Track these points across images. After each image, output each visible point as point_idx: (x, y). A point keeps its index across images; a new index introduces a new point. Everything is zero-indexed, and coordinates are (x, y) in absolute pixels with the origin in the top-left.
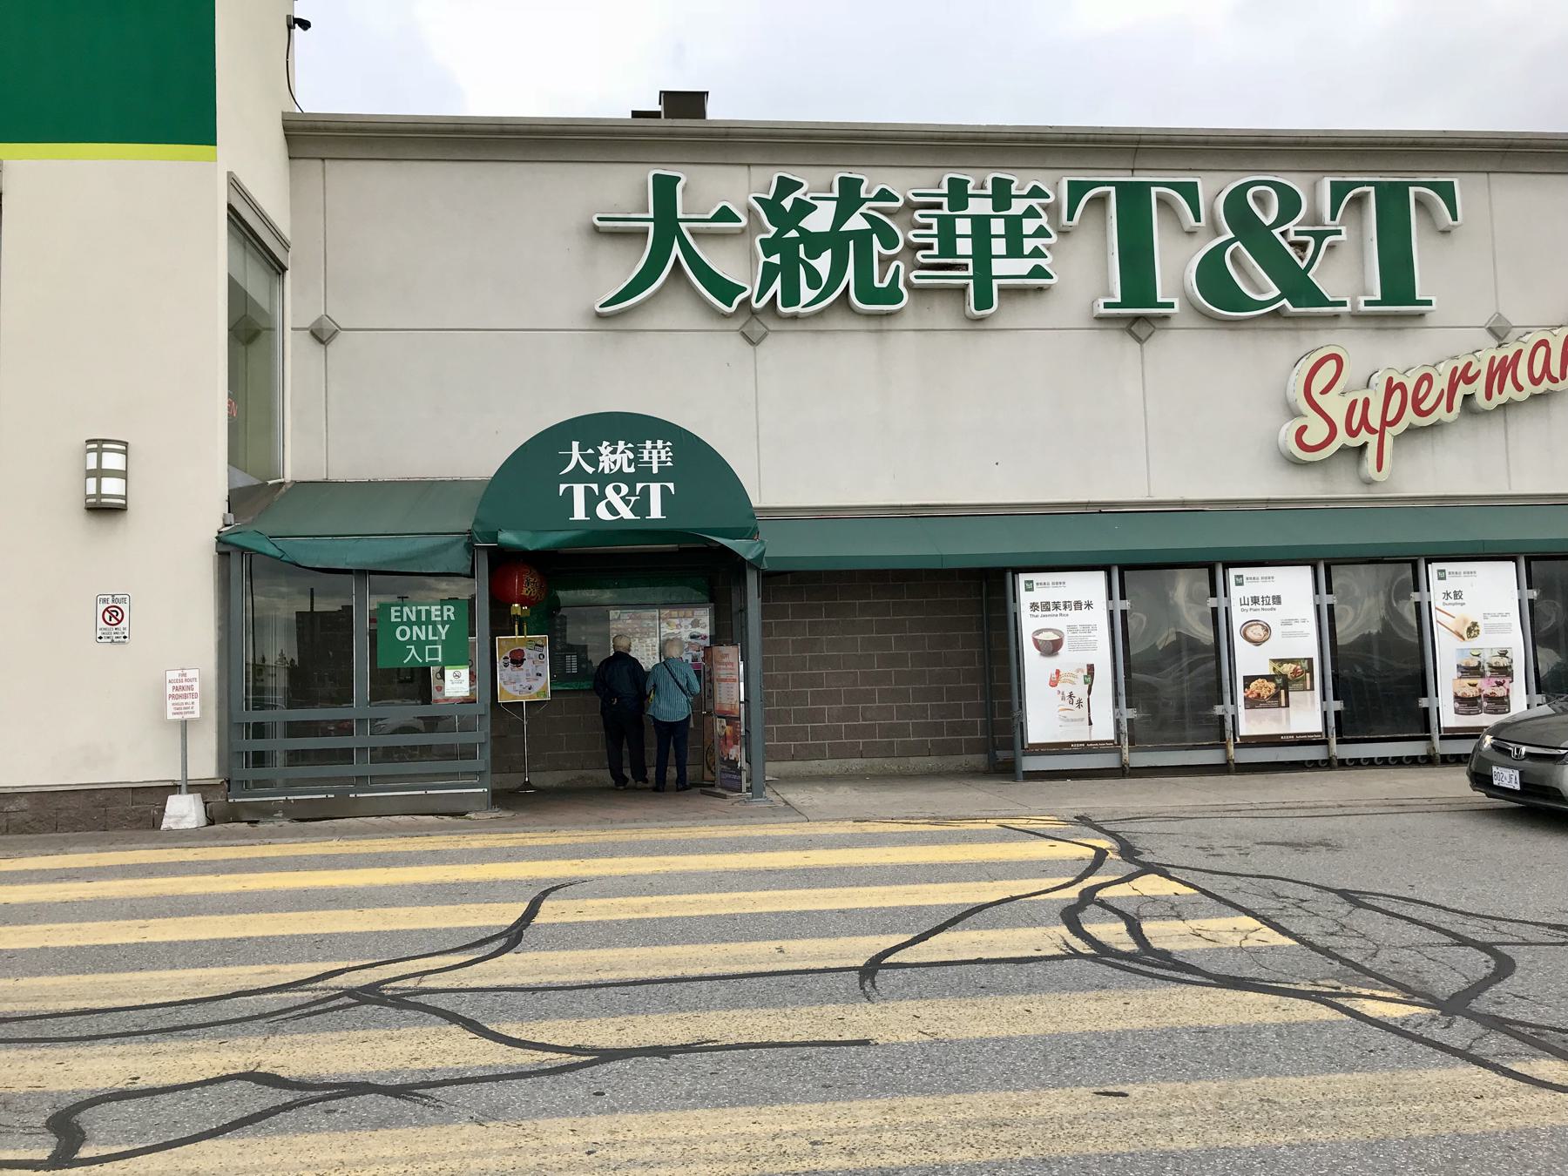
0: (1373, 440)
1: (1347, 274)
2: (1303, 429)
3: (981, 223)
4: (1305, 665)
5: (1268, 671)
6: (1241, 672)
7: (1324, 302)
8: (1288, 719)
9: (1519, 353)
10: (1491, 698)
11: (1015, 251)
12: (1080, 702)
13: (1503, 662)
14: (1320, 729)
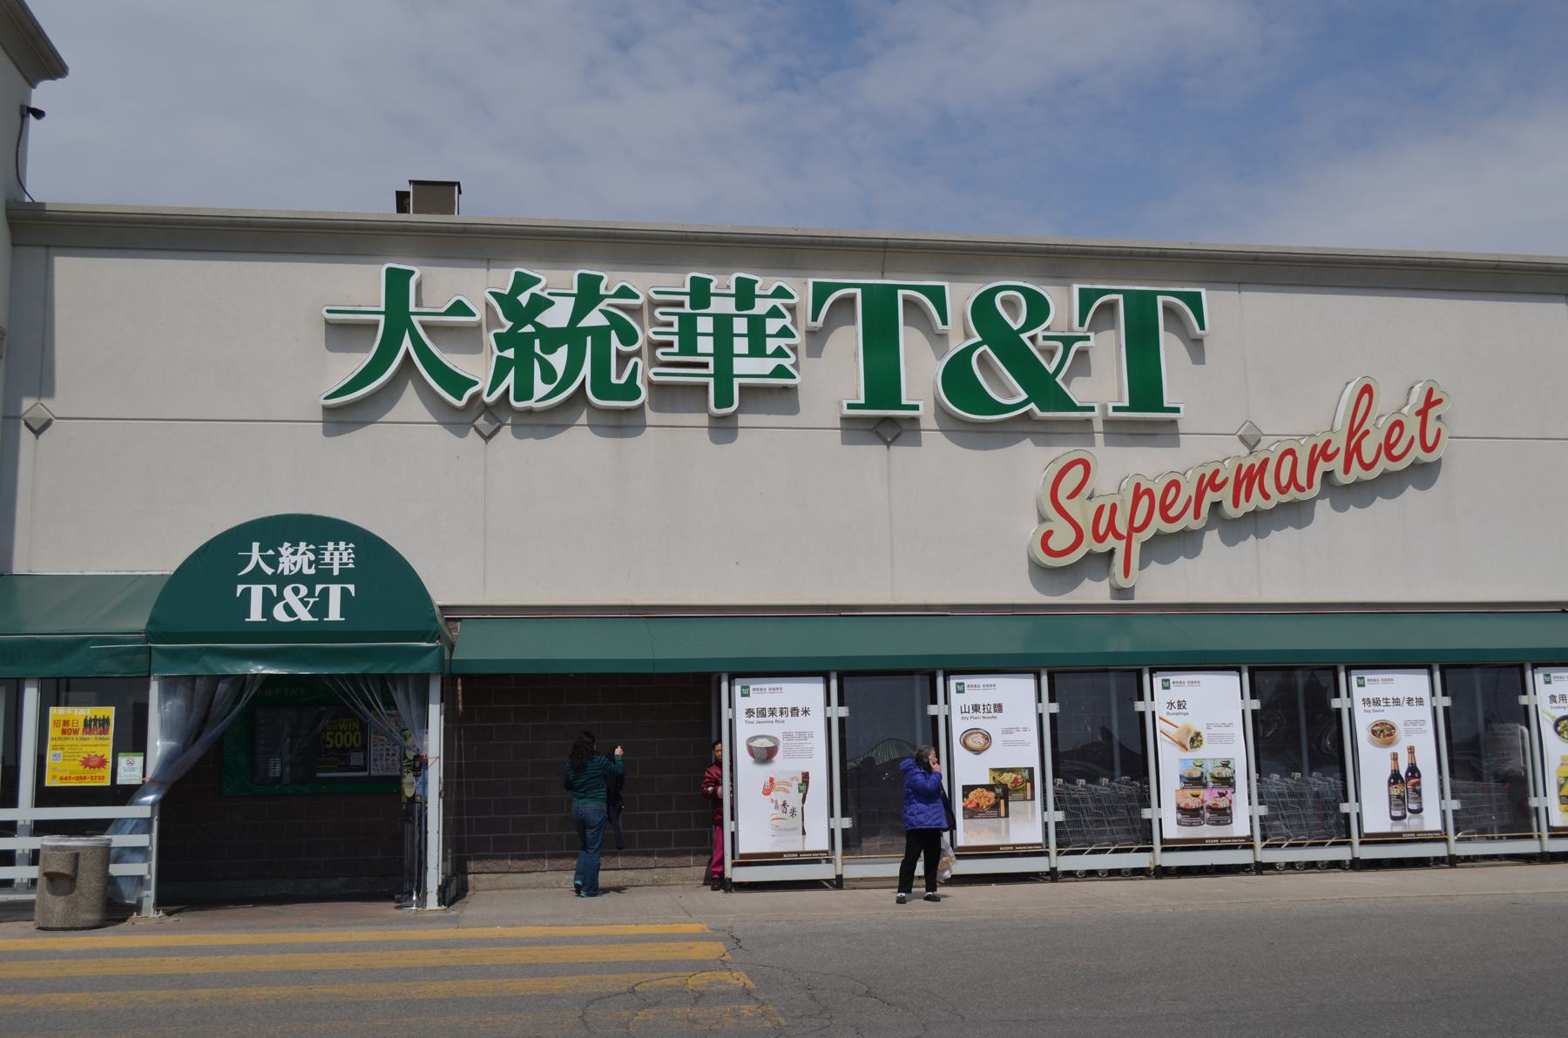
0: (1120, 546)
1: (1102, 385)
2: (1048, 534)
3: (723, 325)
4: (1026, 774)
5: (987, 781)
6: (960, 780)
7: (1074, 408)
8: (1007, 830)
9: (1265, 462)
10: (1214, 810)
11: (757, 350)
12: (793, 812)
13: (1225, 773)
14: (1040, 840)
